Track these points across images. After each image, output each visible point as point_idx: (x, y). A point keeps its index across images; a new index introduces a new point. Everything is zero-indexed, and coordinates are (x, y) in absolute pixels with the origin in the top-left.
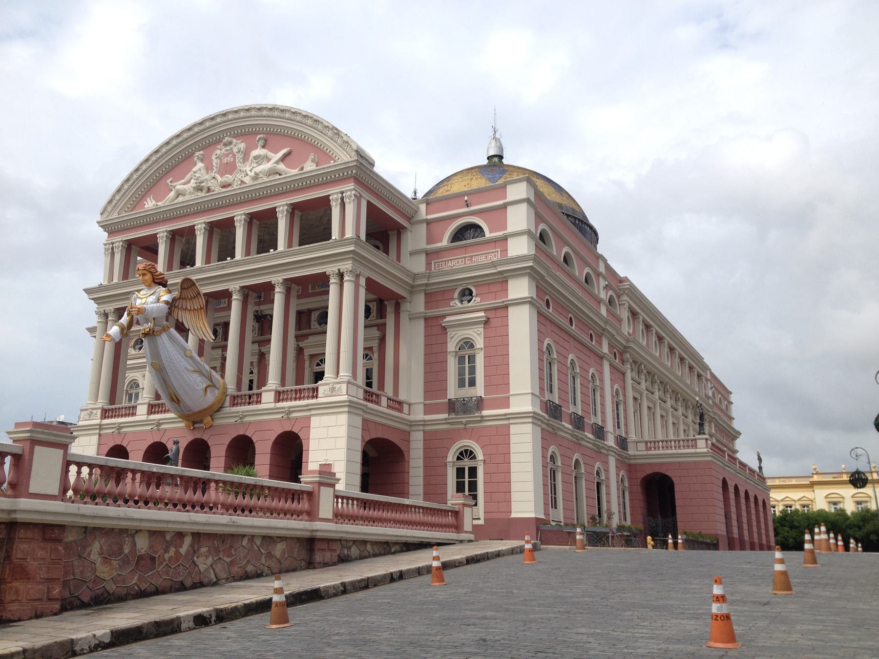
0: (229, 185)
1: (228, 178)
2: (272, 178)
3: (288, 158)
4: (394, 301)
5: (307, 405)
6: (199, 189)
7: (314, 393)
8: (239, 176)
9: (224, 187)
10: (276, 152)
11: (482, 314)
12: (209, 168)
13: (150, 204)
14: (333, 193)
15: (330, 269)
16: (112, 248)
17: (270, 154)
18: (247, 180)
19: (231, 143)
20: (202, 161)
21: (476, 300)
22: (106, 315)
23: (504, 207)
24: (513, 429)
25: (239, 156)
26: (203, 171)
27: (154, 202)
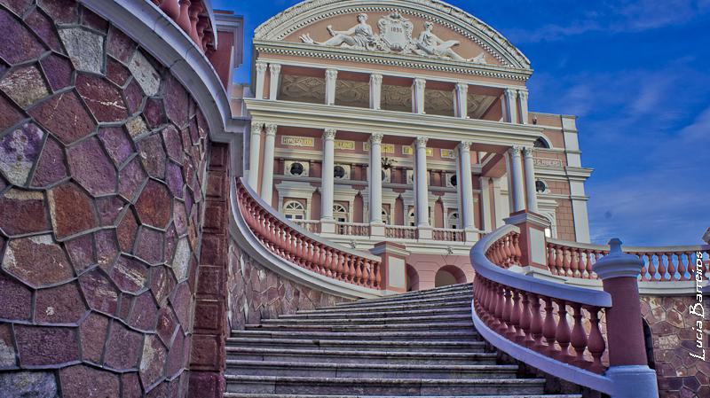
3: (456, 47)
4: (488, 178)
6: (371, 44)
8: (414, 47)
10: (445, 39)
11: (554, 202)
12: (377, 29)
14: (512, 88)
16: (268, 68)
18: (418, 51)
19: (399, 17)
20: (367, 22)
21: (547, 191)
22: (264, 128)
26: (371, 33)
27: (311, 41)
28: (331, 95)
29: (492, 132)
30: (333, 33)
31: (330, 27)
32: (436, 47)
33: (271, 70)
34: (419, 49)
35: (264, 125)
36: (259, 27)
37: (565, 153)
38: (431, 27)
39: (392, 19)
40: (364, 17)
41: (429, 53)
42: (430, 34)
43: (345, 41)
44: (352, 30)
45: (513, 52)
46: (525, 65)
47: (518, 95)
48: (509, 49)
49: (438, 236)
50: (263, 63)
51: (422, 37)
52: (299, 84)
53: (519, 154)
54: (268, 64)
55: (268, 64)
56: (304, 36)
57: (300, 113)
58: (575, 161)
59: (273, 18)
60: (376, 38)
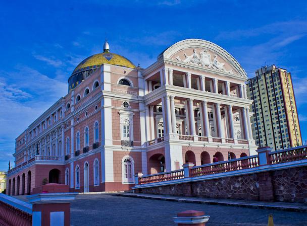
10: (221, 63)
12: (200, 55)
16: (169, 71)
18: (214, 67)
22: (170, 98)
30: (187, 56)
44: (192, 56)
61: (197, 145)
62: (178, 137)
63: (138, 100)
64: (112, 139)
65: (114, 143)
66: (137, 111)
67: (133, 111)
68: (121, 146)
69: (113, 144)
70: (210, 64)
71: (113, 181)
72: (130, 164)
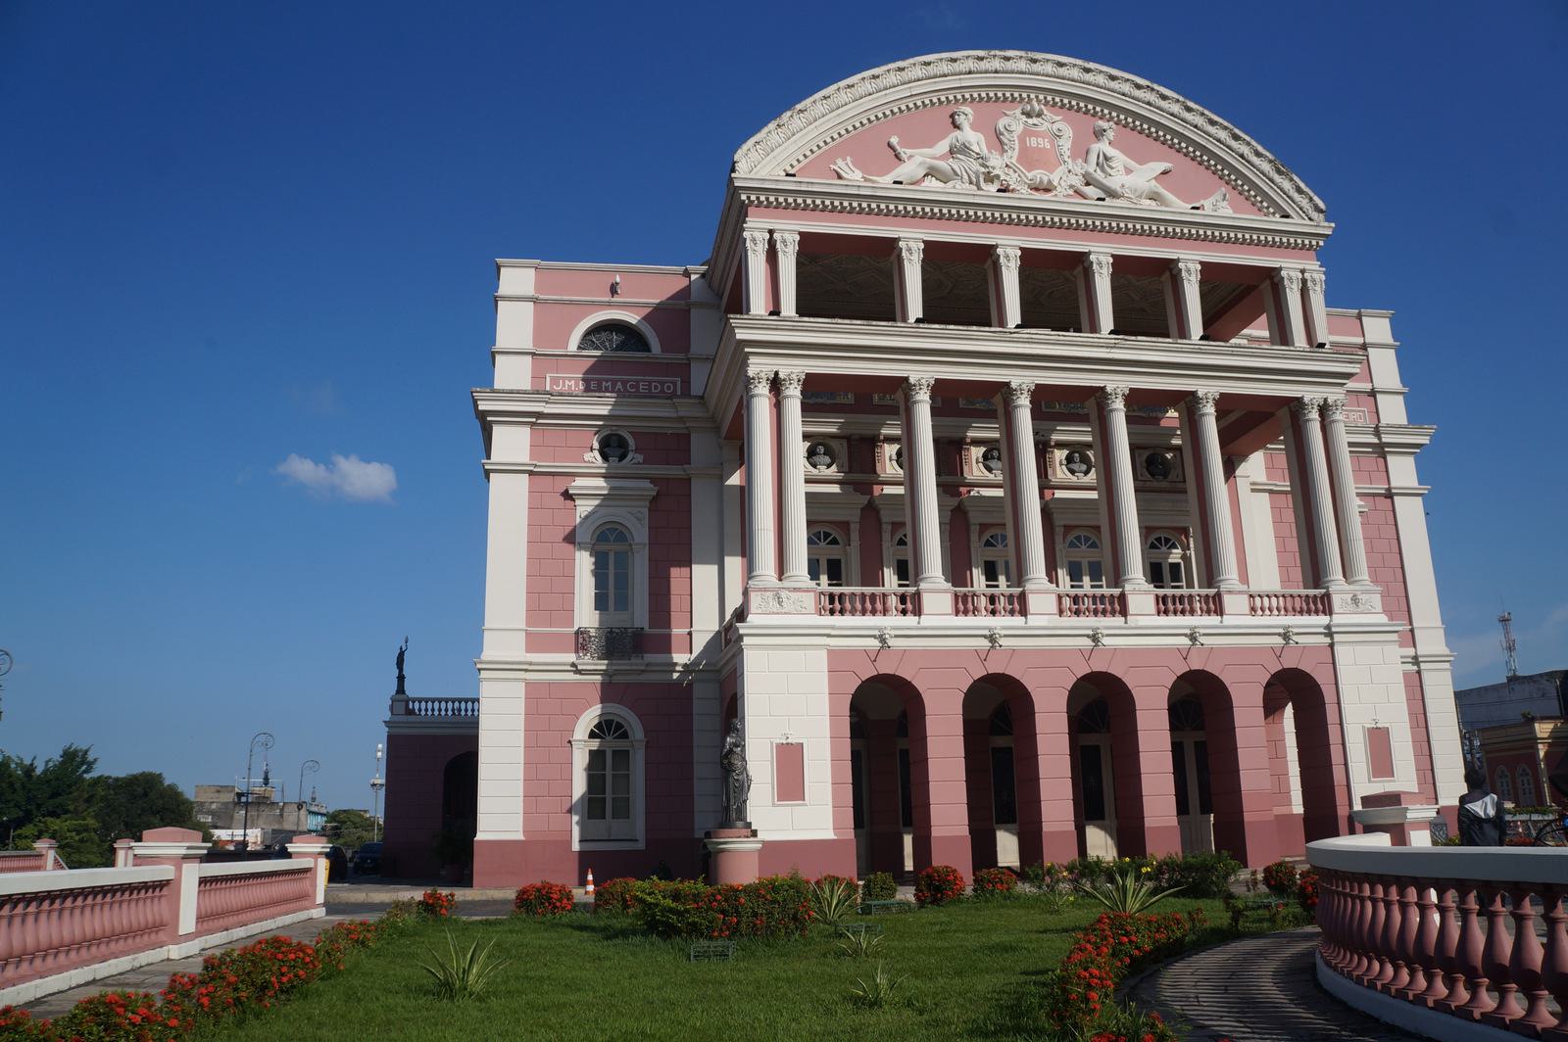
0: (1047, 190)
1: (1039, 175)
2: (1153, 203)
5: (1328, 627)
6: (990, 178)
7: (1324, 605)
9: (1037, 189)
10: (1141, 163)
13: (854, 176)
14: (1291, 267)
15: (1311, 394)
16: (772, 244)
17: (1132, 164)
19: (1039, 115)
20: (974, 128)
22: (776, 384)
23: (1364, 347)
24: (1425, 676)
25: (1066, 144)
28: (915, 307)
29: (1247, 363)
31: (894, 140)
32: (1129, 181)
33: (779, 246)
34: (1088, 184)
35: (776, 373)
36: (745, 147)
37: (1373, 393)
38: (1110, 134)
39: (1024, 118)
40: (967, 114)
41: (1113, 194)
42: (1111, 151)
43: (932, 172)
44: (943, 147)
45: (1287, 185)
46: (1315, 215)
47: (1304, 281)
48: (1277, 178)
49: (1164, 606)
50: (761, 230)
51: (1093, 158)
52: (845, 278)
53: (1314, 414)
54: (771, 232)
55: (771, 232)
56: (840, 162)
57: (854, 348)
58: (1393, 410)
59: (772, 126)
60: (996, 162)
61: (939, 633)
62: (809, 600)
63: (681, 419)
64: (524, 627)
65: (534, 643)
66: (674, 471)
67: (654, 480)
68: (571, 657)
69: (528, 650)
70: (1064, 178)
71: (520, 836)
72: (621, 744)
